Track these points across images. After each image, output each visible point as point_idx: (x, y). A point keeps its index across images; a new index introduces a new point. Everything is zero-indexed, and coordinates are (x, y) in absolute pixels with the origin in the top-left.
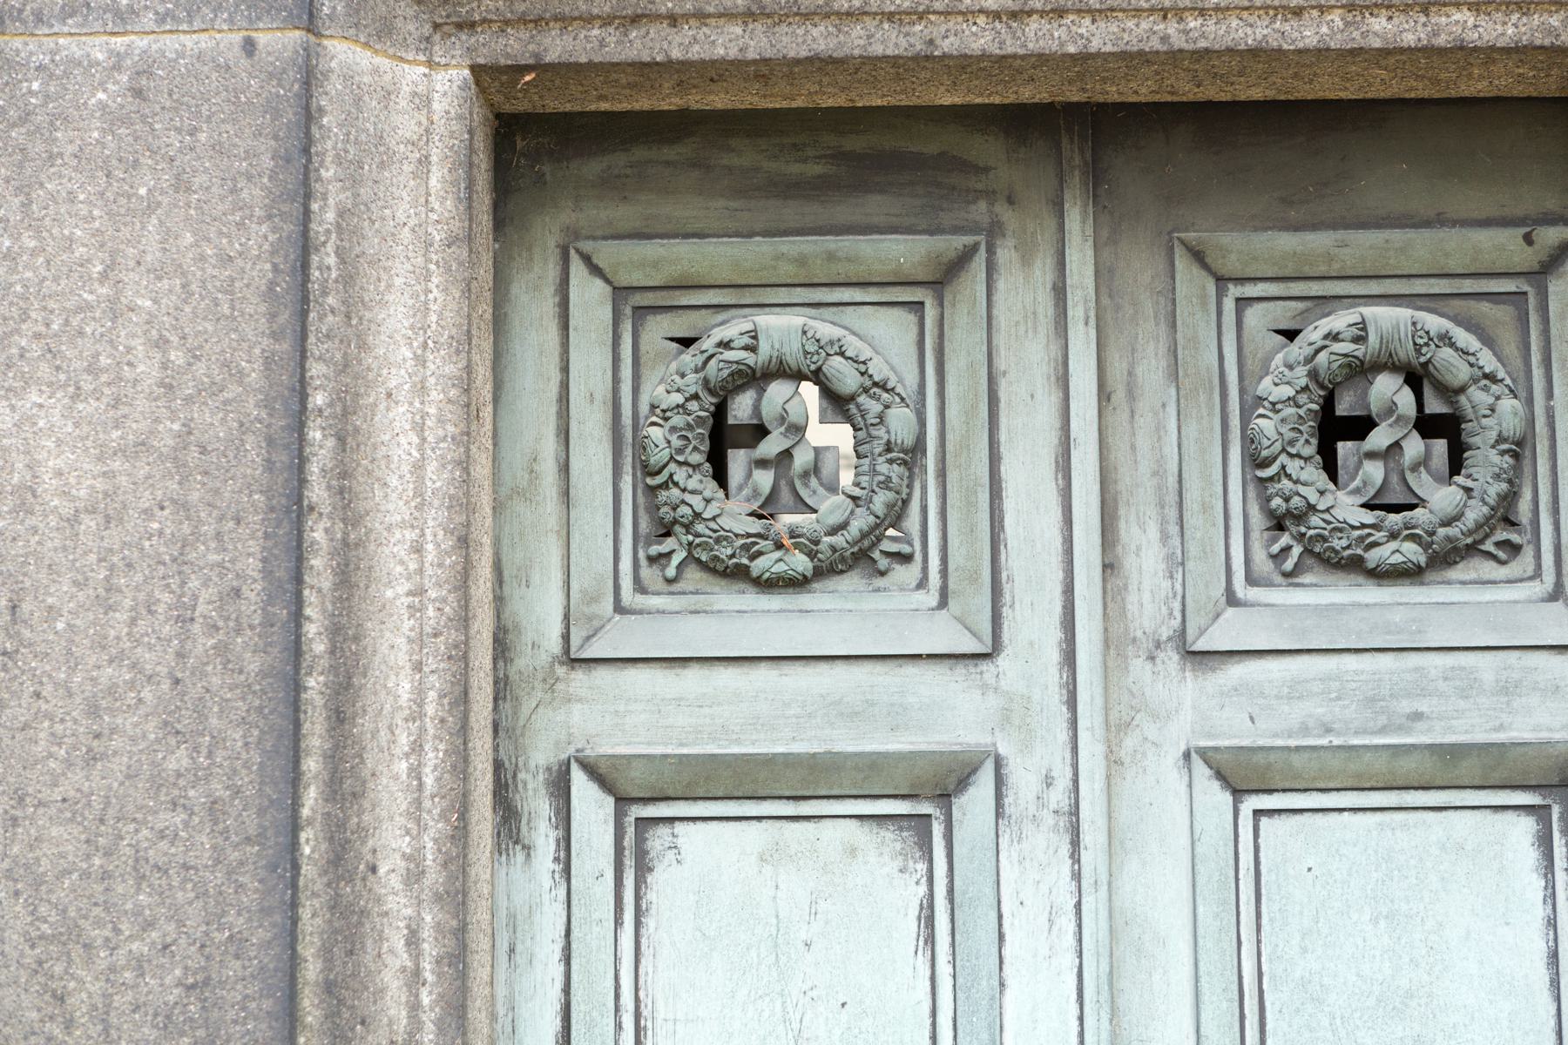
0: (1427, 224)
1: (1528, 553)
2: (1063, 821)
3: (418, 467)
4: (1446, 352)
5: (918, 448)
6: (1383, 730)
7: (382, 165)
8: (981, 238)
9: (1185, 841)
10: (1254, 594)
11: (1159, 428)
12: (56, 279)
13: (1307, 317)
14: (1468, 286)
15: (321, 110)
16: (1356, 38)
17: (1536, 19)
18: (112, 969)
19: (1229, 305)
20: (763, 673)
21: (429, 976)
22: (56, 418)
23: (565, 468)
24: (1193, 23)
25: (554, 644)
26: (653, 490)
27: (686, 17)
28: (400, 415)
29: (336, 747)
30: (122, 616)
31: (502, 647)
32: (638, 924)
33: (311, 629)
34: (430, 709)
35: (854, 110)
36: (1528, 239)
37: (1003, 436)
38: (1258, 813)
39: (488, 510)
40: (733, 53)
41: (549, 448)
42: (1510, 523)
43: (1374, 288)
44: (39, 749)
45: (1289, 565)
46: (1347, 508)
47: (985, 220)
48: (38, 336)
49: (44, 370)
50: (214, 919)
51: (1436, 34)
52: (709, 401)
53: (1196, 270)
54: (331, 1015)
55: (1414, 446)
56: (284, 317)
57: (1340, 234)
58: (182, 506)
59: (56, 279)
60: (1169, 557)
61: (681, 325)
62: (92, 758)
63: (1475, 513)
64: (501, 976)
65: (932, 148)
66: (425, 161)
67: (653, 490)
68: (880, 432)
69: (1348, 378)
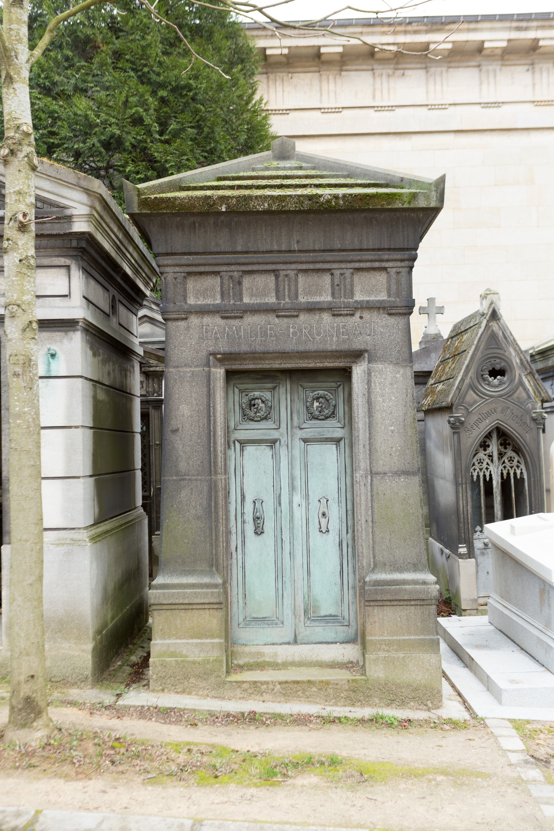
20: (255, 431)
23: (234, 409)
25: (233, 427)
28: (219, 406)
41: (232, 407)
58: (199, 416)
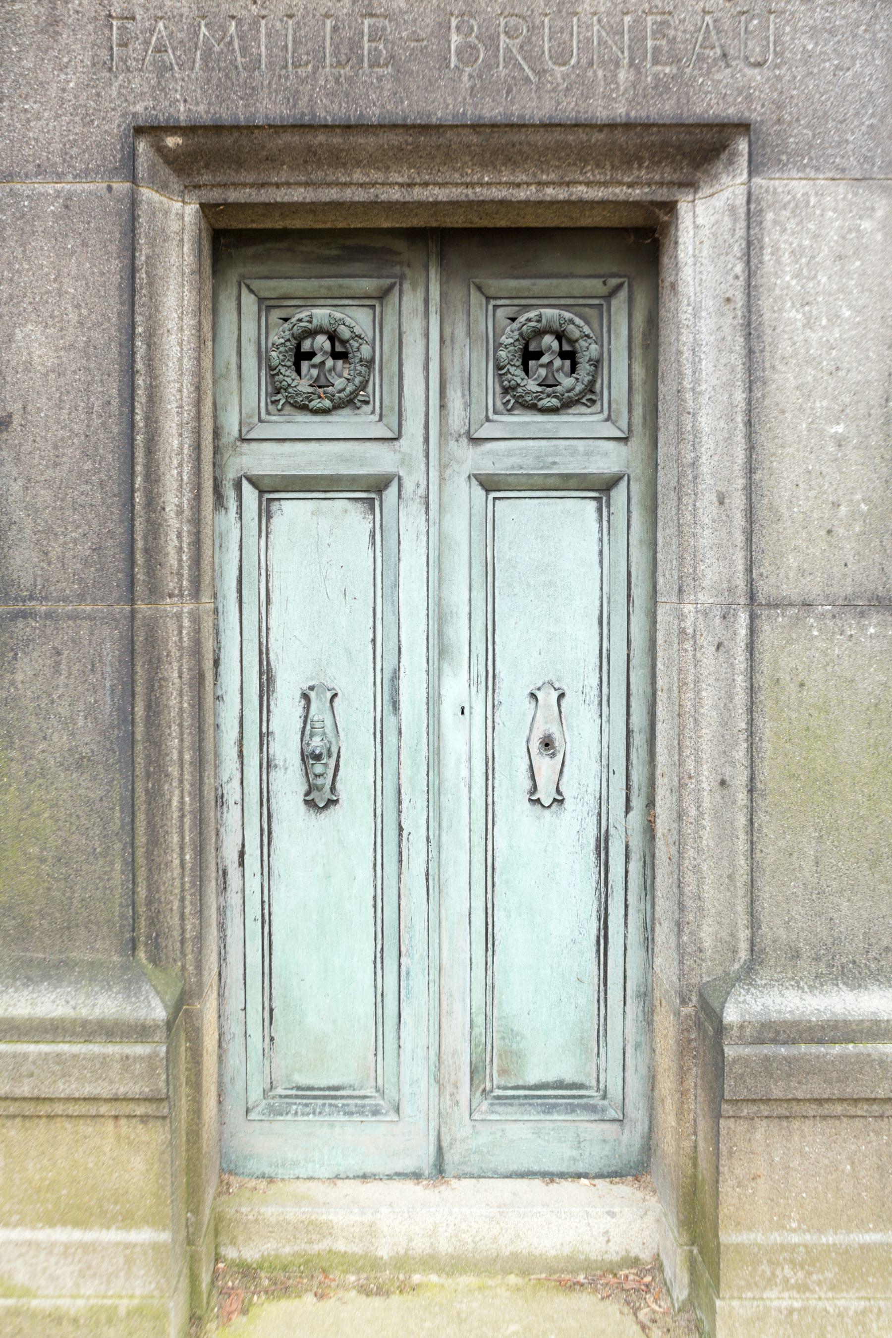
0: (565, 277)
1: (598, 404)
2: (423, 500)
3: (180, 359)
4: (571, 327)
5: (372, 361)
6: (542, 468)
7: (164, 241)
8: (398, 280)
9: (467, 508)
10: (496, 417)
11: (463, 354)
12: (37, 281)
13: (520, 313)
14: (581, 301)
15: (139, 216)
16: (540, 197)
17: (610, 190)
18: (65, 543)
19: (490, 308)
20: (313, 445)
21: (186, 550)
22: (38, 336)
23: (240, 367)
24: (478, 190)
25: (235, 433)
26: (273, 376)
27: (283, 184)
28: (173, 339)
29: (148, 462)
30: (66, 411)
31: (217, 433)
32: (267, 537)
33: (138, 418)
34: (186, 451)
35: (350, 229)
36: (605, 283)
37: (404, 357)
38: (495, 499)
39: (210, 381)
40: (301, 199)
41: (234, 359)
42: (592, 392)
43: (546, 302)
44: (36, 461)
45: (509, 407)
46: (532, 385)
47: (399, 273)
48: (30, 303)
49: (33, 316)
50: (102, 524)
51: (571, 195)
52: (294, 342)
53: (478, 294)
54: (147, 561)
55: (558, 363)
56: (125, 297)
57: (533, 281)
58: (88, 370)
59: (37, 281)
60: (465, 403)
61: (283, 313)
62: (56, 465)
63: (579, 388)
64: (217, 555)
65: (380, 245)
66: (182, 240)
67: (273, 376)
68: (358, 354)
69: (534, 336)
